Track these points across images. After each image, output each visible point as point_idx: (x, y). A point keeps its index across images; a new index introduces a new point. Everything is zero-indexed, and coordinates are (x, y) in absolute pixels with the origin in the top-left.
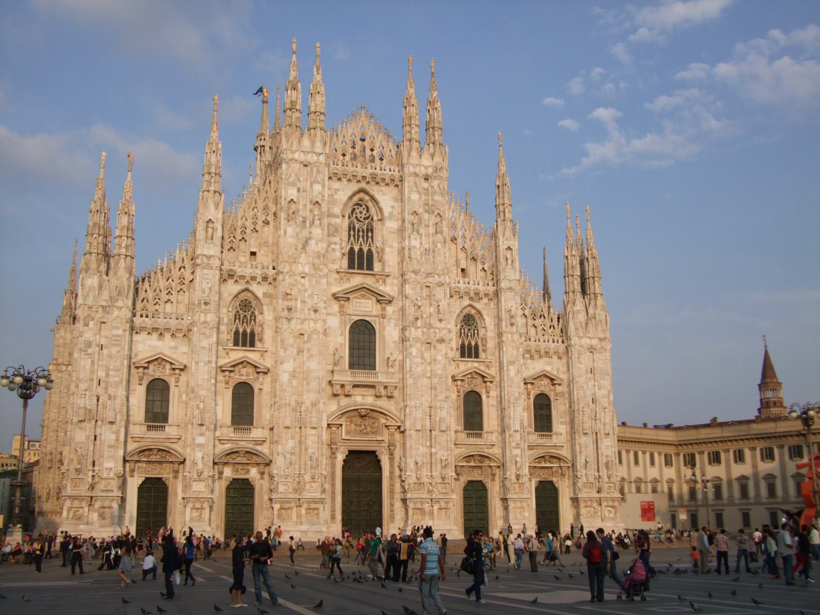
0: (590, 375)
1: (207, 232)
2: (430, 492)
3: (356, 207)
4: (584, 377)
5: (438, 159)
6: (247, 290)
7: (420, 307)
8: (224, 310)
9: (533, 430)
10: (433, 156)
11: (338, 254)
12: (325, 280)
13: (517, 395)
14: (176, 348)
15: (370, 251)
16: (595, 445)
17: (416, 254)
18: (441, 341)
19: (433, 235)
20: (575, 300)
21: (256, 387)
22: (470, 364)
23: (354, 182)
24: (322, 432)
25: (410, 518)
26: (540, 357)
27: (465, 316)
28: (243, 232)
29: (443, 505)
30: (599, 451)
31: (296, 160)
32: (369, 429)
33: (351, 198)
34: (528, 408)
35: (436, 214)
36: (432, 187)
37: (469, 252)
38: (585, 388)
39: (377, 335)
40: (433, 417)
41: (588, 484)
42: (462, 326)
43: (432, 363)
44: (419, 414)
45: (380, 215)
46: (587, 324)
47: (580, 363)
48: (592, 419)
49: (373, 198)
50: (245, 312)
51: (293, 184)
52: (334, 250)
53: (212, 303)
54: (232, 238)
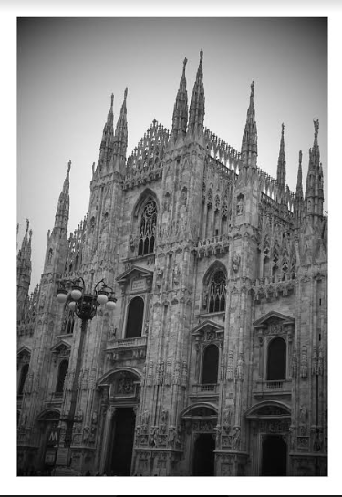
2: (153, 444)
7: (160, 276)
8: (62, 310)
9: (264, 380)
13: (234, 342)
16: (314, 392)
18: (175, 302)
19: (180, 207)
25: (136, 468)
26: (278, 299)
27: (216, 274)
29: (162, 458)
30: (320, 398)
32: (131, 388)
38: (308, 323)
41: (302, 440)
47: (305, 296)
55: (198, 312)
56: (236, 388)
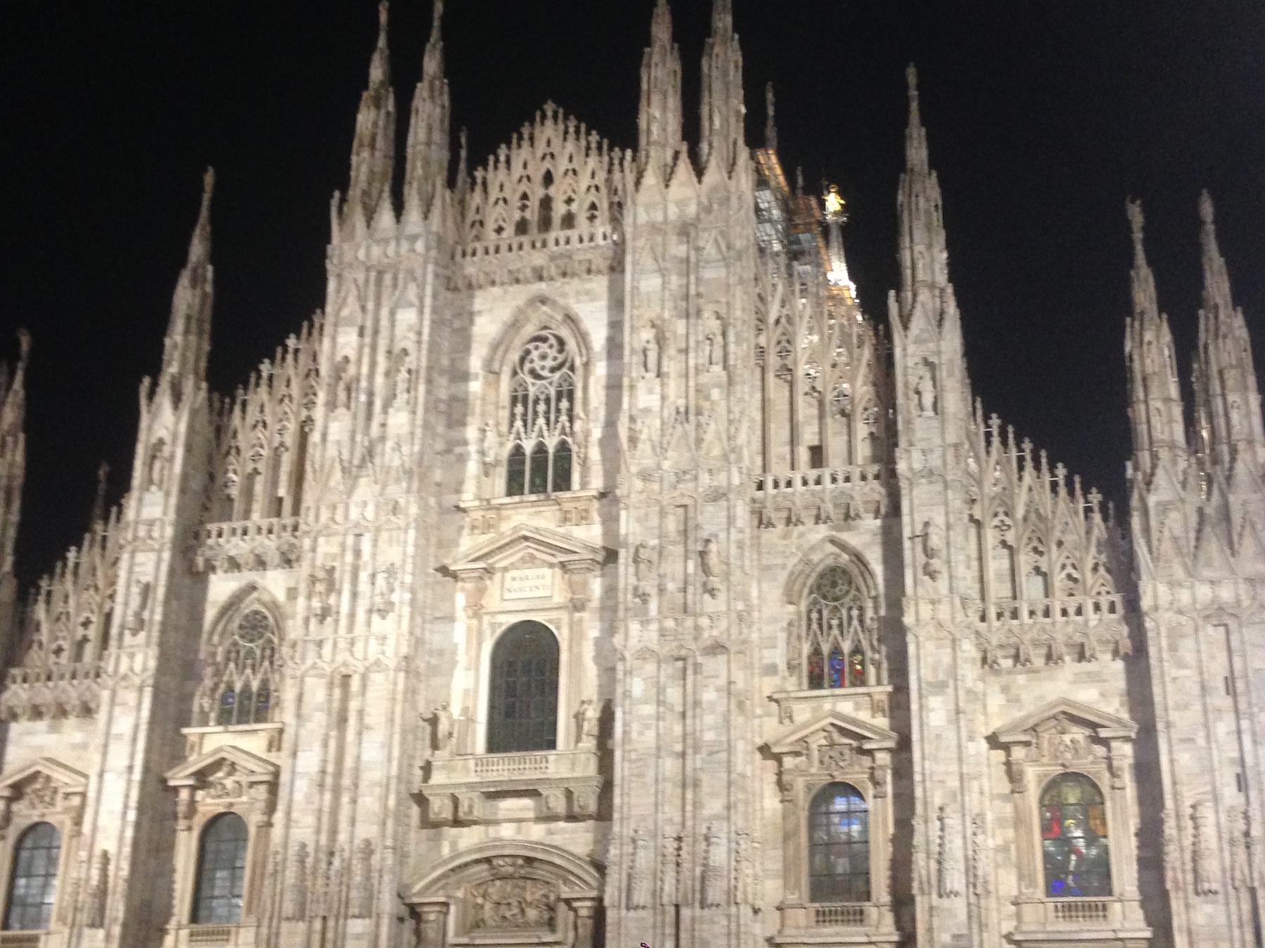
0: (1220, 700)
3: (531, 346)
4: (1198, 707)
5: (713, 174)
6: (253, 588)
10: (699, 171)
11: (473, 467)
12: (412, 534)
13: (954, 783)
14: (84, 746)
15: (563, 448)
17: (650, 429)
18: (717, 648)
20: (1153, 474)
21: (254, 820)
22: (827, 706)
23: (515, 288)
24: (378, 926)
27: (822, 576)
28: (256, 457)
32: (532, 914)
33: (514, 325)
34: (1019, 821)
36: (698, 249)
37: (830, 397)
39: (564, 657)
40: (686, 866)
42: (815, 602)
43: (689, 714)
44: (645, 859)
46: (1198, 539)
47: (1181, 665)
48: (1232, 842)
49: (570, 319)
50: (251, 641)
51: (349, 322)
55: (769, 685)
56: (976, 917)
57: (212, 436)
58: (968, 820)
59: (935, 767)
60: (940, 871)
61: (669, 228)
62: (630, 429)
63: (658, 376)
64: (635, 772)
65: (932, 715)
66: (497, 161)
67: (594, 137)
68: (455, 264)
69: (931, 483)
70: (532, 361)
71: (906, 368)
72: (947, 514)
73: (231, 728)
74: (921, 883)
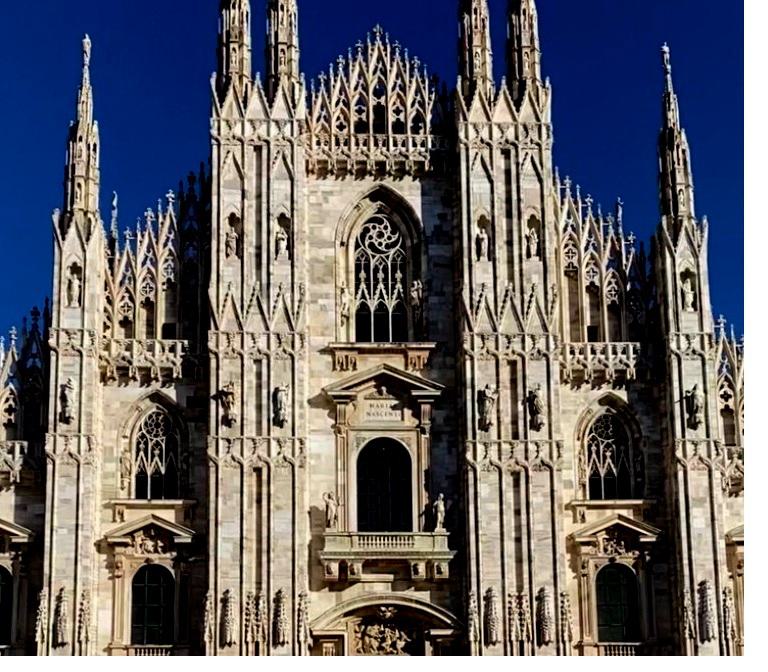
1: (70, 287)
27: (598, 421)
31: (240, 140)
35: (526, 217)
37: (605, 290)
45: (416, 235)
50: (156, 436)
52: (323, 308)
53: (83, 417)
54: (127, 300)
57: (107, 266)
58: (721, 591)
59: (697, 555)
60: (701, 625)
61: (495, 145)
62: (471, 299)
63: (489, 260)
64: (486, 550)
65: (695, 520)
66: (336, 65)
67: (417, 62)
68: (311, 149)
69: (693, 359)
70: (371, 238)
71: (674, 274)
72: (705, 382)
73: (154, 502)
74: (690, 630)
